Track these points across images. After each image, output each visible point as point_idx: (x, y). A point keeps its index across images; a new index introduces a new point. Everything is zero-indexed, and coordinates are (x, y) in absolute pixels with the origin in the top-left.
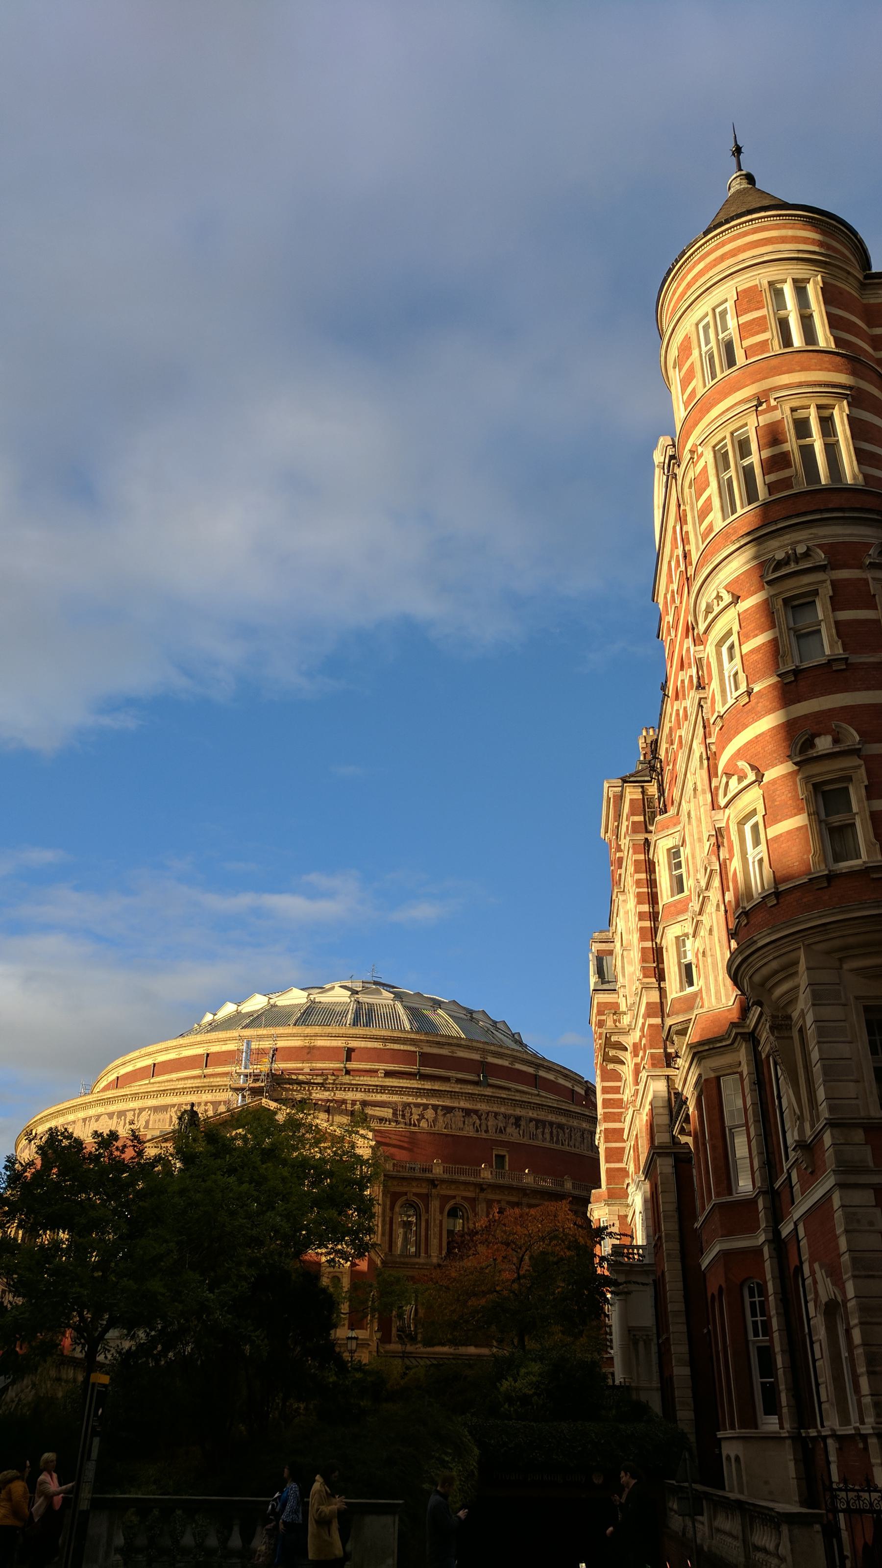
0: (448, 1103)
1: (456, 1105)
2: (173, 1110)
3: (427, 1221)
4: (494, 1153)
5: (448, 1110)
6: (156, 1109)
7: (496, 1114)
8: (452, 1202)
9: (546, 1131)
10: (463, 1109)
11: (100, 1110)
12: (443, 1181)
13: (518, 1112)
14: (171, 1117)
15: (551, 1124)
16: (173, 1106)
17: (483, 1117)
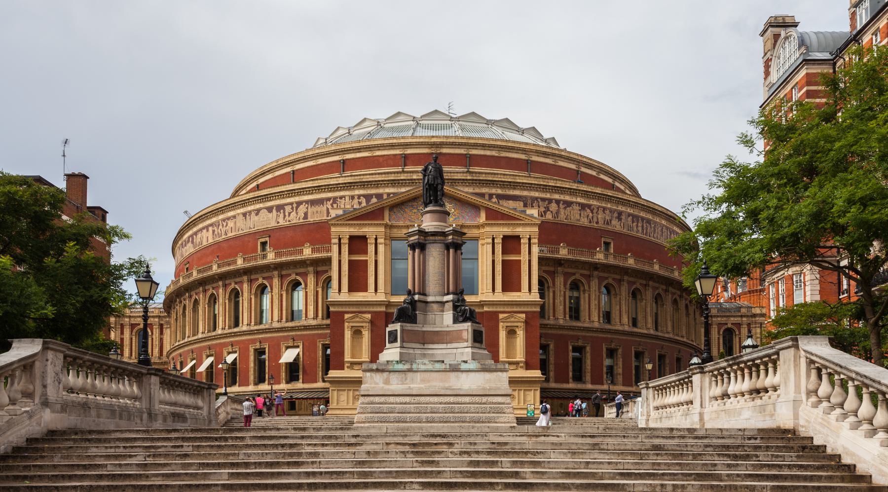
0: (568, 198)
1: (574, 200)
2: (329, 203)
3: (554, 292)
4: (603, 240)
5: (568, 204)
6: (313, 203)
7: (604, 209)
8: (573, 278)
9: (640, 225)
10: (579, 204)
11: (258, 206)
12: (568, 260)
13: (620, 208)
14: (328, 209)
15: (643, 219)
16: (328, 199)
17: (595, 211)
